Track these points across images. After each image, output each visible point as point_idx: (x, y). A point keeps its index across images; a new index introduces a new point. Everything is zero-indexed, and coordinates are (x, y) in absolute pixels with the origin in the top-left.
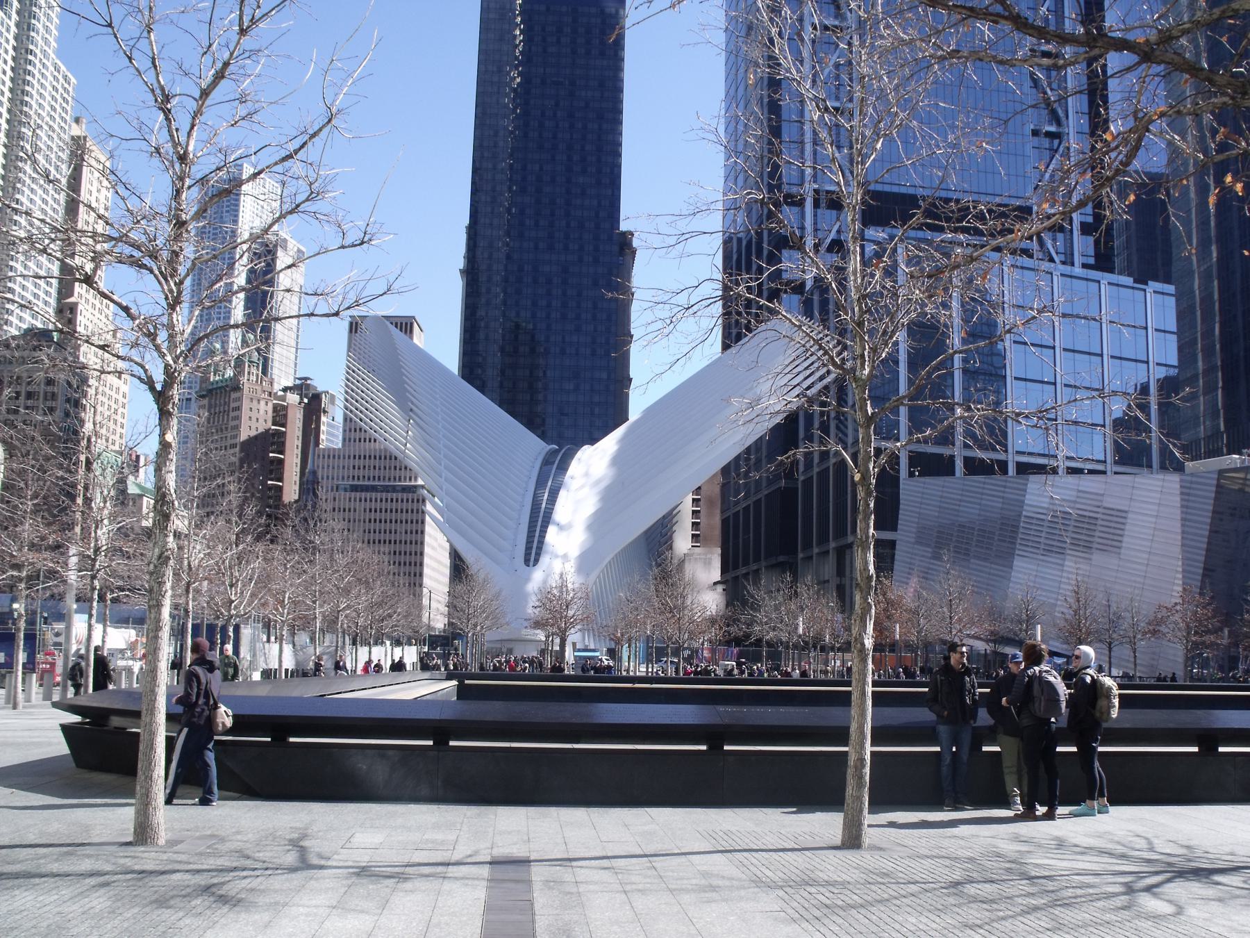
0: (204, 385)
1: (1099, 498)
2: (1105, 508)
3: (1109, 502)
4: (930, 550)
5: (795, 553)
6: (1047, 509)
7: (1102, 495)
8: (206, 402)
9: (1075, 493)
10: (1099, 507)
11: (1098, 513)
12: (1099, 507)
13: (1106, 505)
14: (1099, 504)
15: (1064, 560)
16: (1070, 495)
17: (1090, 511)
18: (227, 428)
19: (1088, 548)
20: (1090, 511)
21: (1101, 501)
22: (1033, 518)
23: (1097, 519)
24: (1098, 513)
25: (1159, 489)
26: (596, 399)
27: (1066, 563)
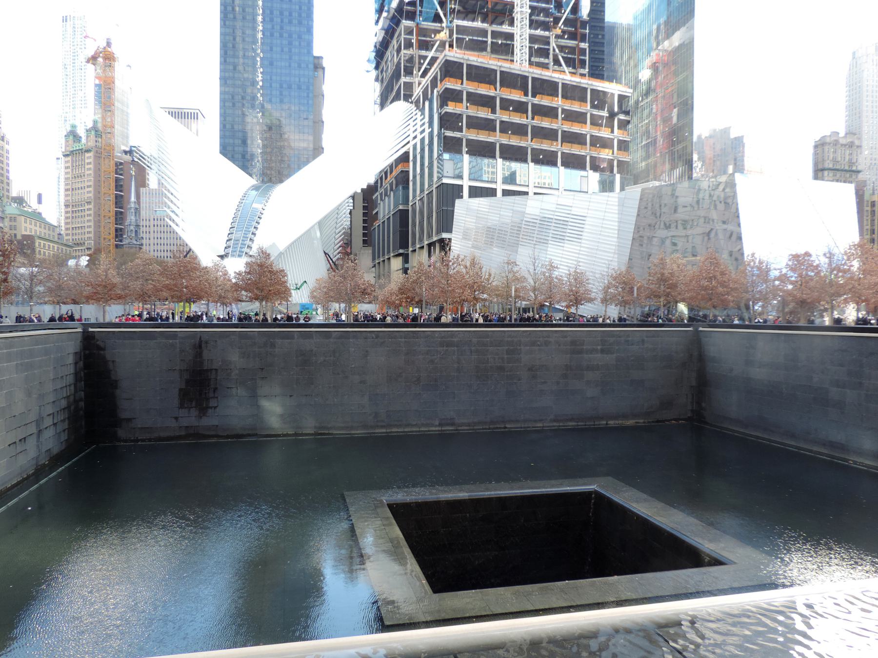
0: (68, 148)
1: (570, 208)
2: (573, 215)
3: (575, 211)
4: (471, 243)
5: (407, 247)
6: (538, 216)
7: (571, 207)
8: (69, 158)
9: (555, 206)
10: (569, 214)
11: (568, 218)
12: (569, 214)
13: (572, 213)
14: (569, 212)
15: (548, 247)
16: (552, 207)
18: (84, 175)
19: (562, 239)
21: (571, 210)
22: (530, 222)
23: (567, 221)
24: (568, 218)
25: (606, 202)
27: (549, 249)
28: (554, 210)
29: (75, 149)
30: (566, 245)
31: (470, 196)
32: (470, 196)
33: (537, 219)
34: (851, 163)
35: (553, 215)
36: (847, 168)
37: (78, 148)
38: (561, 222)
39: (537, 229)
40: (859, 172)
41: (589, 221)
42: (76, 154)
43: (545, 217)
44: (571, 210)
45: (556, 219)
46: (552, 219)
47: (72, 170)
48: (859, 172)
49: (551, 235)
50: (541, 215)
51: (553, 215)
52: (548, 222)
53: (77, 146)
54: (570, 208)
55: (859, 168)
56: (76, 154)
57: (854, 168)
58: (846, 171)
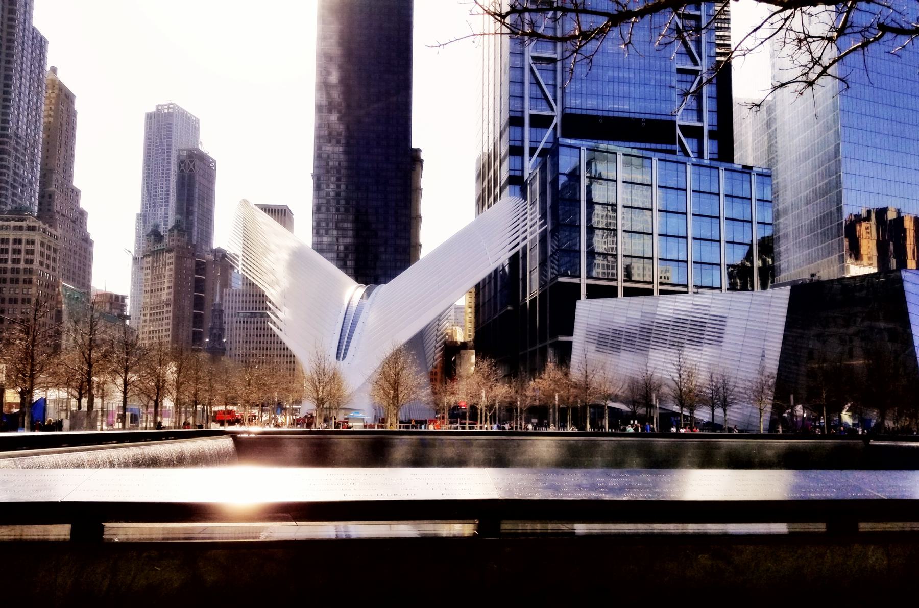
1: (709, 309)
7: (709, 307)
10: (705, 314)
11: (706, 319)
16: (688, 307)
17: (701, 318)
20: (701, 318)
21: (708, 311)
22: (662, 323)
23: (705, 323)
24: (706, 319)
26: (398, 257)
29: (156, 249)
33: (670, 321)
35: (689, 316)
37: (159, 248)
38: (699, 324)
41: (730, 322)
42: (157, 254)
43: (680, 319)
44: (708, 311)
45: (692, 320)
46: (687, 320)
47: (152, 271)
50: (674, 316)
51: (689, 316)
53: (159, 246)
54: (709, 309)
56: (157, 254)
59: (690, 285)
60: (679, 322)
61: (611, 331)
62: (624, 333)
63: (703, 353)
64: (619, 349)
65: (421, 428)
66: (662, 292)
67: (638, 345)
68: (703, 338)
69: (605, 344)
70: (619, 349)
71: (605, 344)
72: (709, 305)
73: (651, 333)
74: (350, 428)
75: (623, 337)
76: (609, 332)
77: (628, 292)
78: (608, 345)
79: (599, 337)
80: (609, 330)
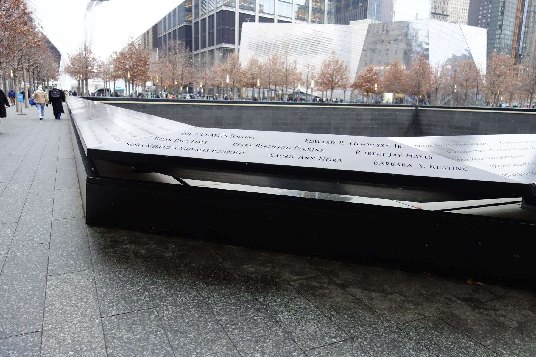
1: (322, 33)
7: (323, 32)
14: (321, 36)
21: (322, 35)
24: (320, 39)
28: (312, 33)
30: (318, 56)
31: (260, 21)
32: (260, 21)
34: (444, 10)
36: (441, 13)
39: (299, 45)
40: (447, 16)
44: (322, 35)
45: (312, 40)
46: (310, 39)
48: (447, 16)
49: (309, 49)
52: (307, 41)
54: (322, 33)
55: (448, 14)
57: (445, 13)
58: (441, 15)
59: (275, 15)
60: (305, 40)
61: (264, 43)
62: (272, 45)
63: (317, 58)
64: (269, 54)
65: (154, 97)
66: (279, 21)
67: (274, 51)
68: (318, 50)
69: (260, 51)
70: (269, 54)
71: (260, 51)
72: (322, 31)
73: (288, 46)
74: (119, 96)
75: (272, 47)
76: (263, 43)
77: (262, 20)
78: (262, 51)
79: (257, 46)
80: (262, 42)
